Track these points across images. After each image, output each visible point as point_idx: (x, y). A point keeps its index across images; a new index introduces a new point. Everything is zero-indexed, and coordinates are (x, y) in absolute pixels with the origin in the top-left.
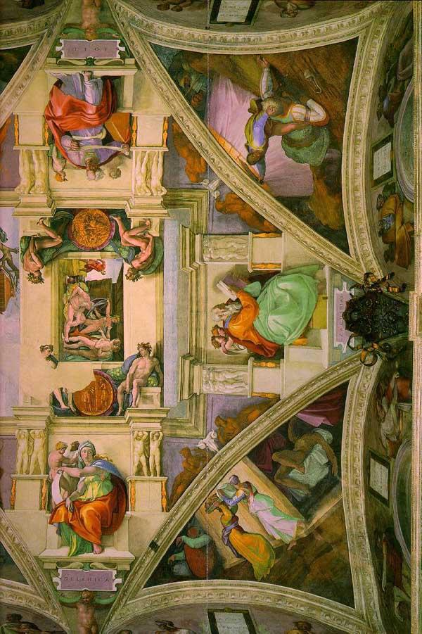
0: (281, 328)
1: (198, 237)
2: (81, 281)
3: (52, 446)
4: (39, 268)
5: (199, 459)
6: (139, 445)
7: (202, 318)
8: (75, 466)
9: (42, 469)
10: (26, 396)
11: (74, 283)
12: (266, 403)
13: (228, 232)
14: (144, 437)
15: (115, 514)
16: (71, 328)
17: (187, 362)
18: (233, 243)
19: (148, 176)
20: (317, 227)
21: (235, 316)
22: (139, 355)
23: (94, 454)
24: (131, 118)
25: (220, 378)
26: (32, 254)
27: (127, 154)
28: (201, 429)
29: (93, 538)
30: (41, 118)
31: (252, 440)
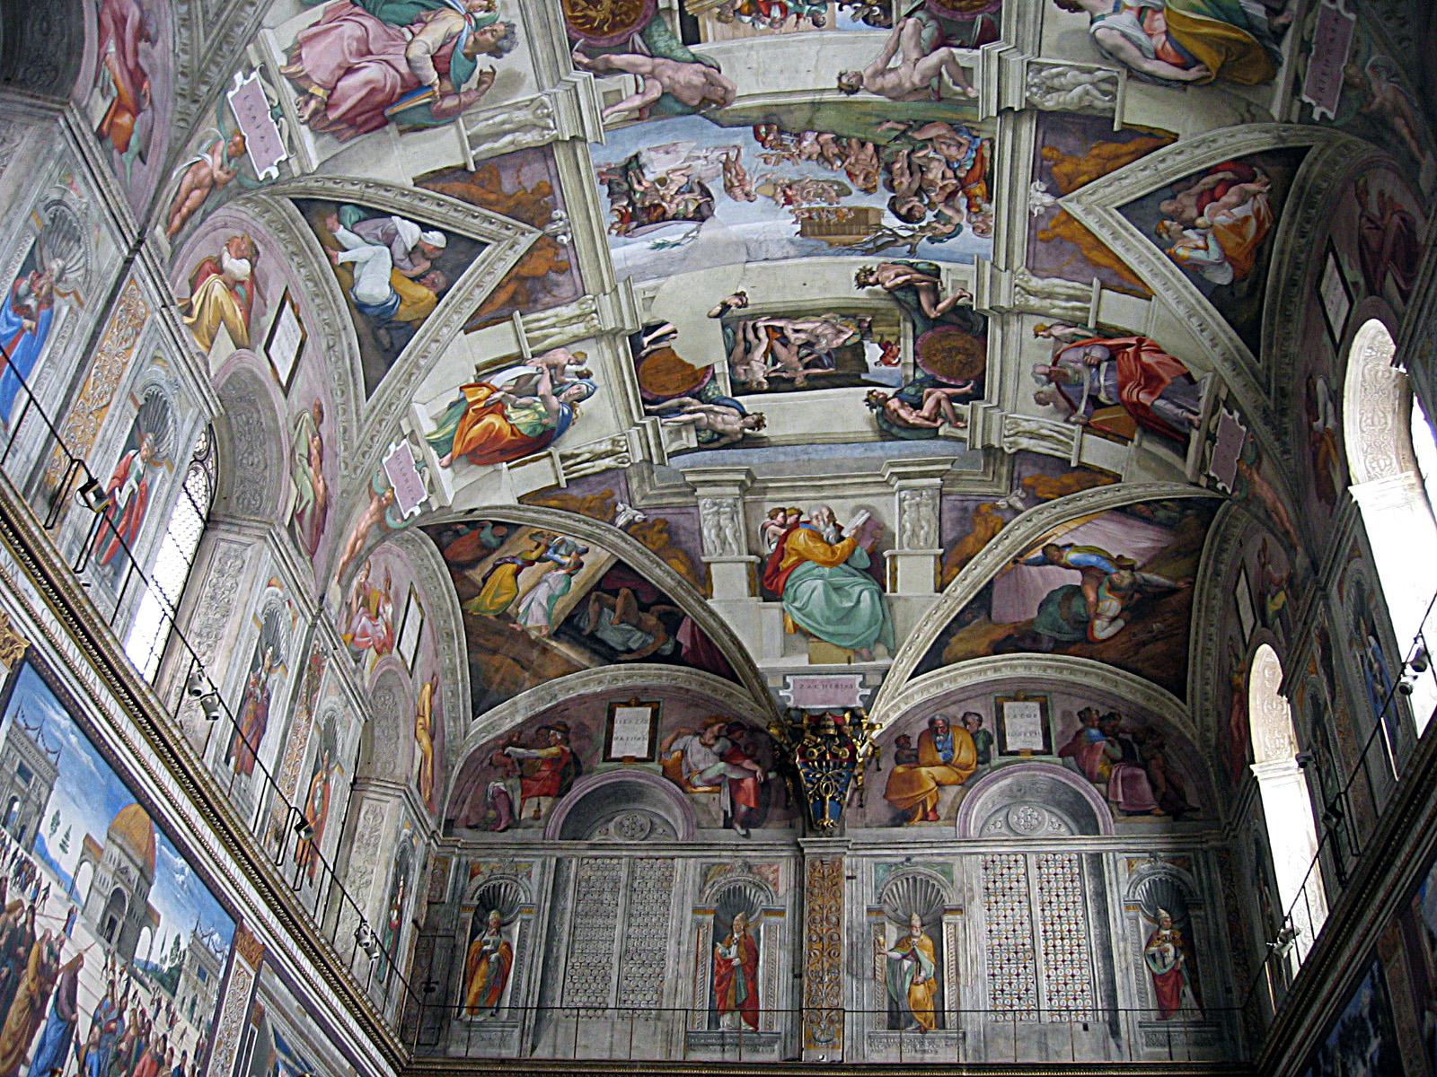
0: (805, 599)
1: (938, 481)
2: (863, 337)
3: (577, 348)
5: (606, 511)
6: (606, 446)
7: (812, 494)
8: (554, 386)
9: (538, 347)
10: (656, 288)
11: (859, 327)
12: (701, 578)
13: (943, 520)
14: (618, 449)
15: (497, 454)
16: (781, 328)
17: (743, 477)
18: (928, 530)
19: (1032, 435)
20: (947, 632)
21: (817, 535)
22: (744, 415)
23: (579, 401)
24: (1124, 440)
25: (724, 521)
26: (908, 277)
27: (1073, 419)
28: (644, 502)
29: (458, 448)
30: (1142, 331)
31: (643, 567)
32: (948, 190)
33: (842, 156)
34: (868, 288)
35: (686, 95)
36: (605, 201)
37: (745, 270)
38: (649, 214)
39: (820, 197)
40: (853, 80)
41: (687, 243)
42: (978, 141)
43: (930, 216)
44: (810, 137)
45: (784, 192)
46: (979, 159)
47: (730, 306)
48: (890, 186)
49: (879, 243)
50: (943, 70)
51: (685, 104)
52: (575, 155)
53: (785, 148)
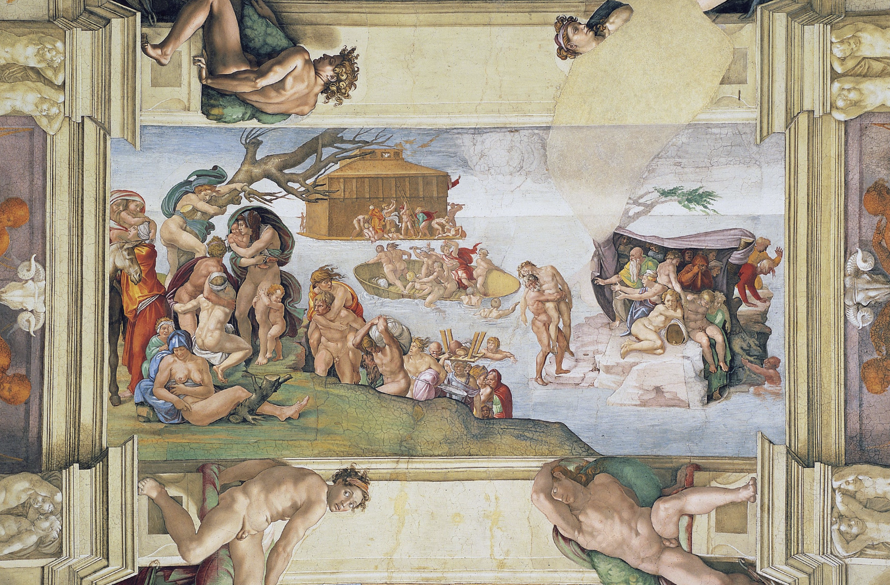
4: (307, 62)
26: (262, 83)
32: (188, 285)
33: (368, 347)
34: (335, 52)
35: (614, 496)
36: (777, 322)
37: (553, 110)
38: (706, 274)
39: (409, 262)
40: (342, 497)
41: (648, 189)
42: (138, 398)
43: (221, 226)
44: (419, 390)
45: (470, 277)
46: (136, 361)
47: (590, 26)
48: (288, 285)
49: (310, 162)
50: (197, 523)
51: (617, 477)
52: (811, 431)
53: (464, 370)
